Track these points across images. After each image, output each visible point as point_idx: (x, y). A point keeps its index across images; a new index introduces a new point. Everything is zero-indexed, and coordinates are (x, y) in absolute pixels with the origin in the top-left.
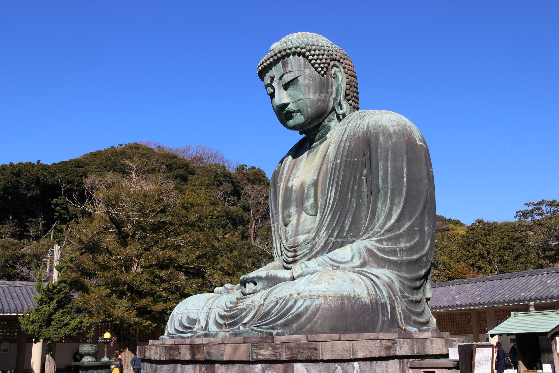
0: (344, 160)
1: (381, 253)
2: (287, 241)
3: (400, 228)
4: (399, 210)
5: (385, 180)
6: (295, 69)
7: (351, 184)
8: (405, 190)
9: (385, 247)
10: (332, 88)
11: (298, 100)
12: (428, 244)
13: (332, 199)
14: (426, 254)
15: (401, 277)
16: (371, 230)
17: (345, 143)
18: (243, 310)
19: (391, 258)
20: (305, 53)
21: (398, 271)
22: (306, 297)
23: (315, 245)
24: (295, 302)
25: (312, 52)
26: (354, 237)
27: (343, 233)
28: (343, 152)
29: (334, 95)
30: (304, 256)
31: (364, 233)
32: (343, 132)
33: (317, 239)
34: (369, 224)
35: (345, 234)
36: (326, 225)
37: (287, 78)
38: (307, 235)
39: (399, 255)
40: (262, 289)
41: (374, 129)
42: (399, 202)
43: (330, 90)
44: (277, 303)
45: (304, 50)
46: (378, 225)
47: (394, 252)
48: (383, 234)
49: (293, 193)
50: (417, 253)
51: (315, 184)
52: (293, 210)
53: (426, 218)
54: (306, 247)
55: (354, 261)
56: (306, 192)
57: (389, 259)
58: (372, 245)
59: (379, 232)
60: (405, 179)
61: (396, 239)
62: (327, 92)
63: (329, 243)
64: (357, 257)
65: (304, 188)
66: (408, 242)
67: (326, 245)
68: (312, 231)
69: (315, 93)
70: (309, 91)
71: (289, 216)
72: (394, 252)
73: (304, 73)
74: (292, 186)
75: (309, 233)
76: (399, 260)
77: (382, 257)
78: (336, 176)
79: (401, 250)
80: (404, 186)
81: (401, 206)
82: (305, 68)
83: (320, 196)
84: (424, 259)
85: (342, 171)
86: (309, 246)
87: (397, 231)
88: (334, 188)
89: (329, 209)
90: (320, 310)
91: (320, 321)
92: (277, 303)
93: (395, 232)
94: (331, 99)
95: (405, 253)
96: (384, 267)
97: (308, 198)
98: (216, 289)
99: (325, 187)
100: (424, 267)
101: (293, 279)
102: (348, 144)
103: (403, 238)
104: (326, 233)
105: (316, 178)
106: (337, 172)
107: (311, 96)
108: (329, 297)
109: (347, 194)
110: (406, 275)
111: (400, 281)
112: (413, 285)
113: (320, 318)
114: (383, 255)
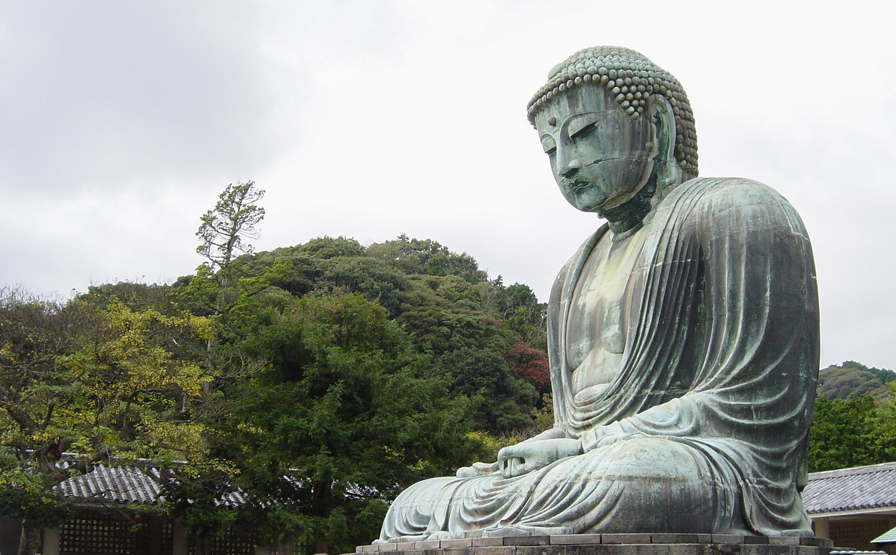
0: (670, 261)
1: (725, 412)
3: (758, 374)
4: (757, 345)
5: (734, 296)
6: (589, 109)
7: (681, 301)
8: (767, 311)
9: (732, 403)
10: (652, 140)
11: (595, 162)
12: (804, 399)
13: (649, 325)
14: (800, 416)
15: (756, 451)
16: (711, 377)
18: (501, 502)
19: (740, 421)
20: (606, 83)
21: (752, 442)
22: (601, 478)
24: (584, 486)
25: (620, 81)
27: (665, 382)
29: (655, 153)
30: (601, 419)
31: (700, 382)
33: (622, 391)
34: (707, 367)
35: (668, 383)
37: (576, 126)
38: (607, 385)
39: (754, 416)
40: (532, 469)
41: (720, 211)
42: (758, 331)
43: (648, 144)
44: (556, 488)
45: (605, 77)
46: (722, 369)
47: (746, 412)
48: (730, 383)
50: (783, 414)
52: (584, 344)
53: (802, 357)
54: (605, 404)
55: (681, 426)
56: (606, 315)
57: (738, 424)
58: (712, 401)
59: (722, 379)
60: (768, 294)
61: (749, 392)
62: (644, 148)
63: (643, 397)
65: (603, 308)
66: (770, 396)
67: (636, 400)
69: (622, 151)
70: (613, 145)
71: (579, 354)
72: (746, 412)
73: (605, 117)
74: (584, 305)
75: (609, 381)
76: (753, 425)
77: (726, 420)
79: (758, 409)
80: (765, 305)
81: (761, 337)
82: (607, 108)
83: (628, 320)
84: (796, 423)
85: (665, 281)
86: (611, 402)
87: (753, 378)
88: (652, 308)
89: (644, 342)
90: (622, 498)
91: (621, 514)
92: (556, 488)
93: (750, 379)
94: (650, 159)
95: (765, 414)
96: (729, 435)
97: (609, 324)
99: (638, 303)
100: (796, 437)
101: (581, 452)
102: (675, 234)
103: (761, 389)
104: (637, 380)
107: (616, 155)
108: (637, 478)
109: (674, 318)
110: (764, 449)
111: (754, 458)
112: (774, 464)
113: (621, 510)
114: (728, 417)
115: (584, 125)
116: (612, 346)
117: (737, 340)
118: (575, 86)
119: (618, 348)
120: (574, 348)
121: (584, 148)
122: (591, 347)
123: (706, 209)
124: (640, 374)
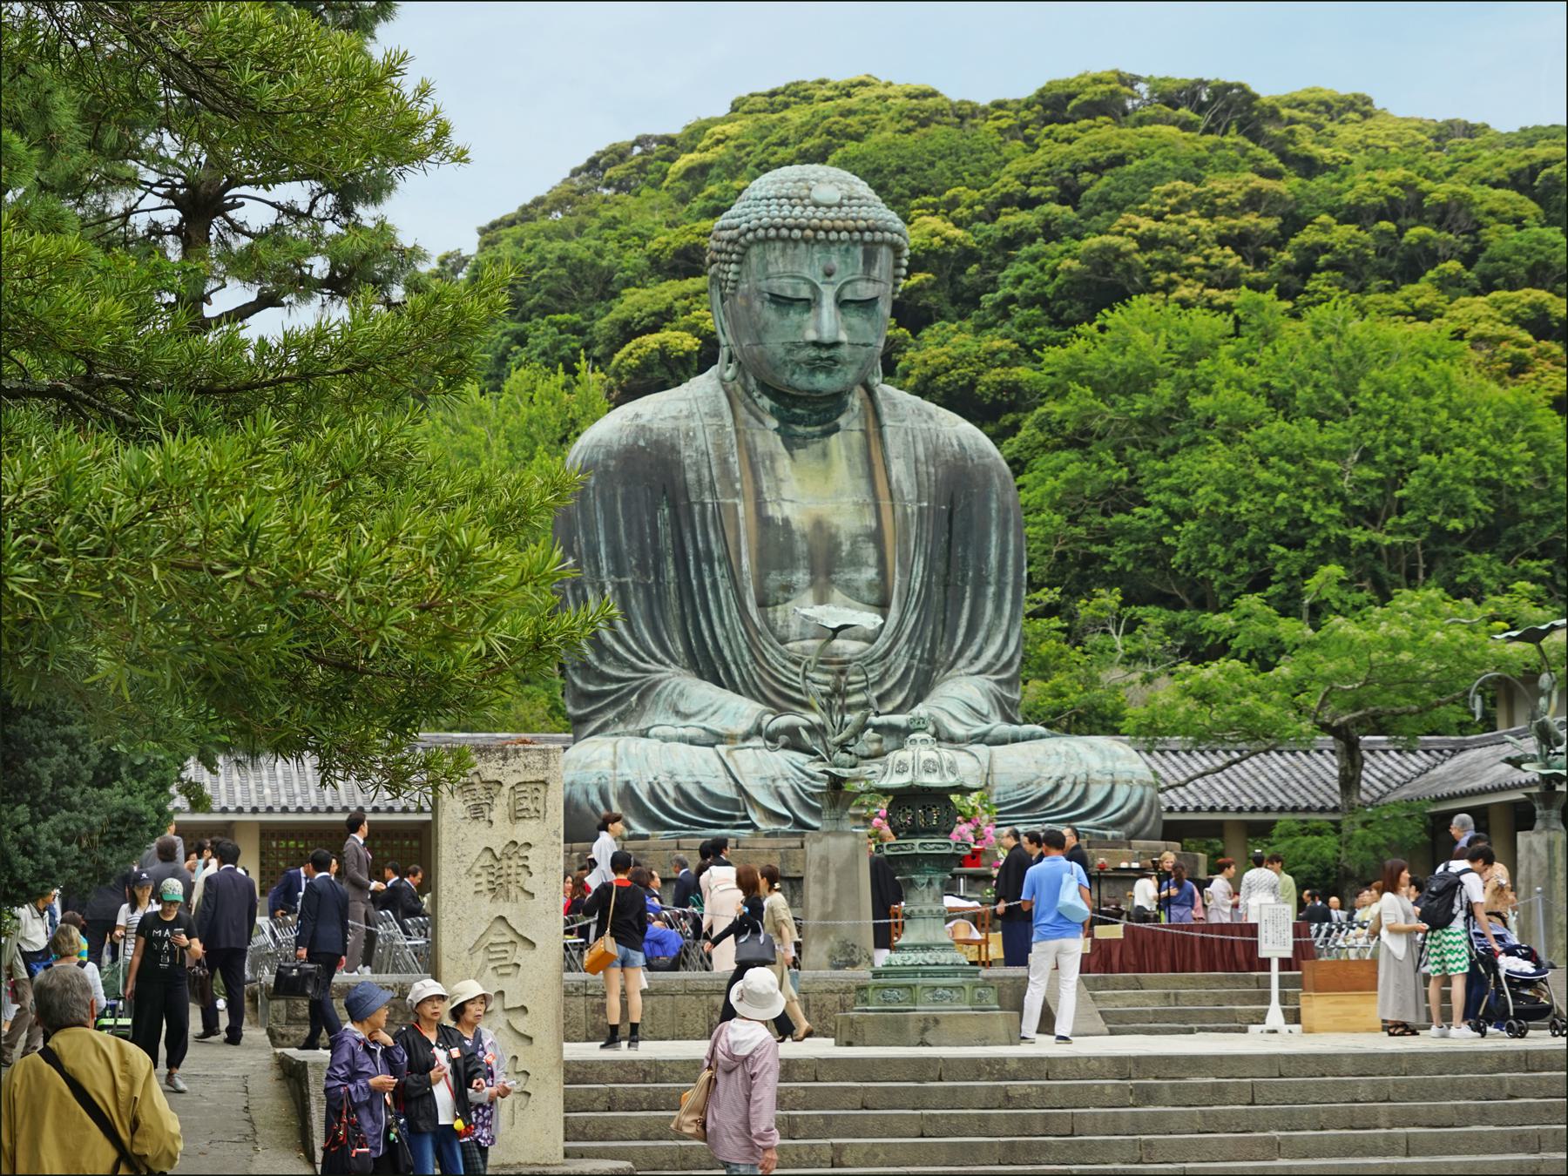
2: (783, 641)
24: (1113, 788)
26: (929, 662)
36: (908, 631)
37: (865, 291)
38: (865, 644)
44: (1057, 787)
49: (797, 537)
51: (877, 537)
56: (846, 547)
68: (881, 639)
71: (788, 588)
74: (786, 521)
92: (1057, 787)
99: (907, 551)
102: (932, 470)
105: (874, 524)
115: (873, 295)
116: (865, 594)
117: (1005, 622)
118: (883, 242)
119: (874, 597)
120: (775, 579)
121: (856, 320)
122: (812, 584)
124: (909, 641)
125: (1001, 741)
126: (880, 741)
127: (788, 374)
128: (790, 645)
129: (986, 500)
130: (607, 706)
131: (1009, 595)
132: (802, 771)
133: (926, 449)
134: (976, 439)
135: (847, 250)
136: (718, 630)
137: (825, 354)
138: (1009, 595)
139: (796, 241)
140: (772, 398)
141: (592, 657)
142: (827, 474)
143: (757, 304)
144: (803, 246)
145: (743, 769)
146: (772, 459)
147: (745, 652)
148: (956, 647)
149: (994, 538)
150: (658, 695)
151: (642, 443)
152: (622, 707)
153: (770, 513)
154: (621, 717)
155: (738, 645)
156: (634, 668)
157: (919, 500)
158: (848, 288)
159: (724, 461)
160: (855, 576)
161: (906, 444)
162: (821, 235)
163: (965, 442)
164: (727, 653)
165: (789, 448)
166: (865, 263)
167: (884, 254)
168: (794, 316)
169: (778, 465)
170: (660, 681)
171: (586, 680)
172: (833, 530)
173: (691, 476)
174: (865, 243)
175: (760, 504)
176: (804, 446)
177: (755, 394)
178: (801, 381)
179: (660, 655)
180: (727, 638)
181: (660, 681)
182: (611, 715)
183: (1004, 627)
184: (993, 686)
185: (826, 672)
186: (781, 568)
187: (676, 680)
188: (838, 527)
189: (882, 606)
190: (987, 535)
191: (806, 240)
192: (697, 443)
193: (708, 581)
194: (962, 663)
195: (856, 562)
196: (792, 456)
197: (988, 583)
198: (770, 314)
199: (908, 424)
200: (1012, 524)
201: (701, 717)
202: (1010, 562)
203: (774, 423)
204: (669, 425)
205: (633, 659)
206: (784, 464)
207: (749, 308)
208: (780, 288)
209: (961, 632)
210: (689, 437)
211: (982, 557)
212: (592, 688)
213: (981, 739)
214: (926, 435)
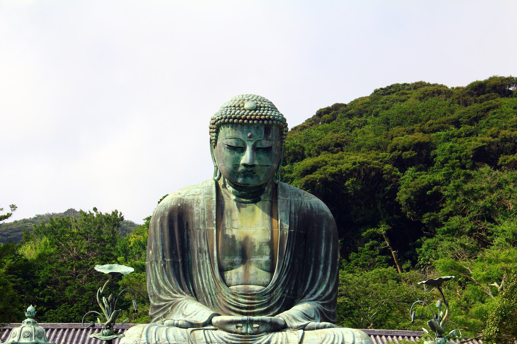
2: (229, 286)
4: (334, 283)
17: (295, 215)
23: (273, 297)
28: (295, 224)
32: (289, 204)
33: (274, 293)
34: (309, 288)
36: (282, 282)
37: (265, 144)
41: (319, 212)
42: (333, 276)
49: (237, 243)
51: (271, 244)
54: (265, 298)
56: (257, 247)
59: (321, 297)
64: (316, 316)
66: (334, 308)
74: (233, 237)
78: (291, 243)
88: (289, 253)
98: (167, 322)
102: (297, 217)
104: (281, 289)
105: (270, 238)
106: (292, 240)
115: (270, 146)
116: (264, 267)
117: (327, 279)
119: (268, 268)
121: (262, 156)
123: (309, 208)
124: (282, 286)
125: (312, 329)
126: (258, 328)
127: (235, 177)
128: (232, 287)
129: (320, 230)
130: (160, 311)
131: (329, 269)
132: (223, 340)
133: (295, 208)
134: (318, 204)
135: (258, 128)
136: (204, 281)
137: (249, 169)
138: (329, 269)
139: (237, 124)
140: (233, 187)
141: (156, 291)
142: (253, 218)
143: (223, 149)
144: (239, 126)
145: (197, 338)
146: (231, 211)
147: (213, 290)
148: (306, 289)
149: (323, 245)
150: (178, 307)
151: (179, 205)
152: (165, 312)
153: (227, 233)
154: (164, 316)
155: (211, 287)
156: (172, 297)
157: (290, 229)
158: (259, 143)
159: (210, 212)
160: (261, 259)
161: (287, 206)
162: (245, 121)
163: (313, 206)
164: (207, 290)
165: (239, 207)
166: (265, 133)
167: (274, 130)
168: (236, 154)
169: (233, 214)
170: (180, 301)
171: (154, 301)
172: (253, 241)
173: (196, 218)
174: (265, 125)
175: (224, 230)
176: (245, 207)
177: (227, 186)
178: (240, 180)
179: (181, 291)
180: (206, 284)
181: (180, 301)
182: (161, 315)
183: (327, 282)
184: (319, 306)
185: (245, 298)
186: (230, 255)
187: (186, 301)
188: (255, 239)
189: (271, 271)
190: (321, 244)
191: (241, 124)
192: (201, 205)
193: (201, 261)
194: (308, 296)
195: (261, 253)
196: (239, 211)
197: (321, 263)
198: (227, 153)
199: (289, 198)
200: (332, 239)
201: (190, 316)
202: (331, 255)
203: (233, 197)
204: (191, 198)
205: (171, 293)
206: (236, 214)
207: (220, 151)
208: (231, 143)
209: (308, 283)
210: (198, 202)
211: (318, 252)
212: (156, 304)
213: (304, 328)
214: (296, 202)
